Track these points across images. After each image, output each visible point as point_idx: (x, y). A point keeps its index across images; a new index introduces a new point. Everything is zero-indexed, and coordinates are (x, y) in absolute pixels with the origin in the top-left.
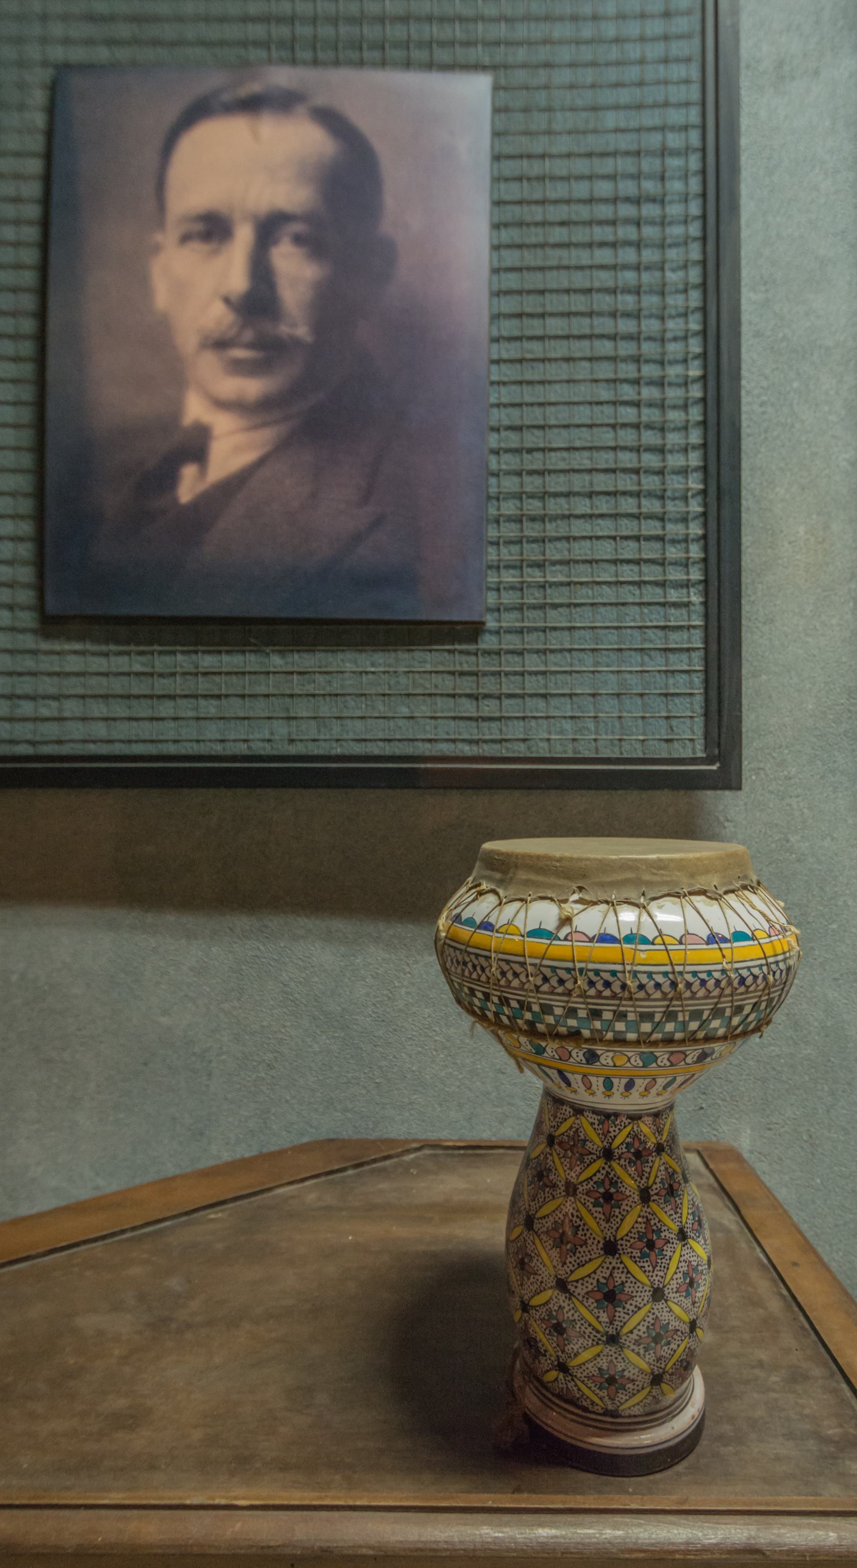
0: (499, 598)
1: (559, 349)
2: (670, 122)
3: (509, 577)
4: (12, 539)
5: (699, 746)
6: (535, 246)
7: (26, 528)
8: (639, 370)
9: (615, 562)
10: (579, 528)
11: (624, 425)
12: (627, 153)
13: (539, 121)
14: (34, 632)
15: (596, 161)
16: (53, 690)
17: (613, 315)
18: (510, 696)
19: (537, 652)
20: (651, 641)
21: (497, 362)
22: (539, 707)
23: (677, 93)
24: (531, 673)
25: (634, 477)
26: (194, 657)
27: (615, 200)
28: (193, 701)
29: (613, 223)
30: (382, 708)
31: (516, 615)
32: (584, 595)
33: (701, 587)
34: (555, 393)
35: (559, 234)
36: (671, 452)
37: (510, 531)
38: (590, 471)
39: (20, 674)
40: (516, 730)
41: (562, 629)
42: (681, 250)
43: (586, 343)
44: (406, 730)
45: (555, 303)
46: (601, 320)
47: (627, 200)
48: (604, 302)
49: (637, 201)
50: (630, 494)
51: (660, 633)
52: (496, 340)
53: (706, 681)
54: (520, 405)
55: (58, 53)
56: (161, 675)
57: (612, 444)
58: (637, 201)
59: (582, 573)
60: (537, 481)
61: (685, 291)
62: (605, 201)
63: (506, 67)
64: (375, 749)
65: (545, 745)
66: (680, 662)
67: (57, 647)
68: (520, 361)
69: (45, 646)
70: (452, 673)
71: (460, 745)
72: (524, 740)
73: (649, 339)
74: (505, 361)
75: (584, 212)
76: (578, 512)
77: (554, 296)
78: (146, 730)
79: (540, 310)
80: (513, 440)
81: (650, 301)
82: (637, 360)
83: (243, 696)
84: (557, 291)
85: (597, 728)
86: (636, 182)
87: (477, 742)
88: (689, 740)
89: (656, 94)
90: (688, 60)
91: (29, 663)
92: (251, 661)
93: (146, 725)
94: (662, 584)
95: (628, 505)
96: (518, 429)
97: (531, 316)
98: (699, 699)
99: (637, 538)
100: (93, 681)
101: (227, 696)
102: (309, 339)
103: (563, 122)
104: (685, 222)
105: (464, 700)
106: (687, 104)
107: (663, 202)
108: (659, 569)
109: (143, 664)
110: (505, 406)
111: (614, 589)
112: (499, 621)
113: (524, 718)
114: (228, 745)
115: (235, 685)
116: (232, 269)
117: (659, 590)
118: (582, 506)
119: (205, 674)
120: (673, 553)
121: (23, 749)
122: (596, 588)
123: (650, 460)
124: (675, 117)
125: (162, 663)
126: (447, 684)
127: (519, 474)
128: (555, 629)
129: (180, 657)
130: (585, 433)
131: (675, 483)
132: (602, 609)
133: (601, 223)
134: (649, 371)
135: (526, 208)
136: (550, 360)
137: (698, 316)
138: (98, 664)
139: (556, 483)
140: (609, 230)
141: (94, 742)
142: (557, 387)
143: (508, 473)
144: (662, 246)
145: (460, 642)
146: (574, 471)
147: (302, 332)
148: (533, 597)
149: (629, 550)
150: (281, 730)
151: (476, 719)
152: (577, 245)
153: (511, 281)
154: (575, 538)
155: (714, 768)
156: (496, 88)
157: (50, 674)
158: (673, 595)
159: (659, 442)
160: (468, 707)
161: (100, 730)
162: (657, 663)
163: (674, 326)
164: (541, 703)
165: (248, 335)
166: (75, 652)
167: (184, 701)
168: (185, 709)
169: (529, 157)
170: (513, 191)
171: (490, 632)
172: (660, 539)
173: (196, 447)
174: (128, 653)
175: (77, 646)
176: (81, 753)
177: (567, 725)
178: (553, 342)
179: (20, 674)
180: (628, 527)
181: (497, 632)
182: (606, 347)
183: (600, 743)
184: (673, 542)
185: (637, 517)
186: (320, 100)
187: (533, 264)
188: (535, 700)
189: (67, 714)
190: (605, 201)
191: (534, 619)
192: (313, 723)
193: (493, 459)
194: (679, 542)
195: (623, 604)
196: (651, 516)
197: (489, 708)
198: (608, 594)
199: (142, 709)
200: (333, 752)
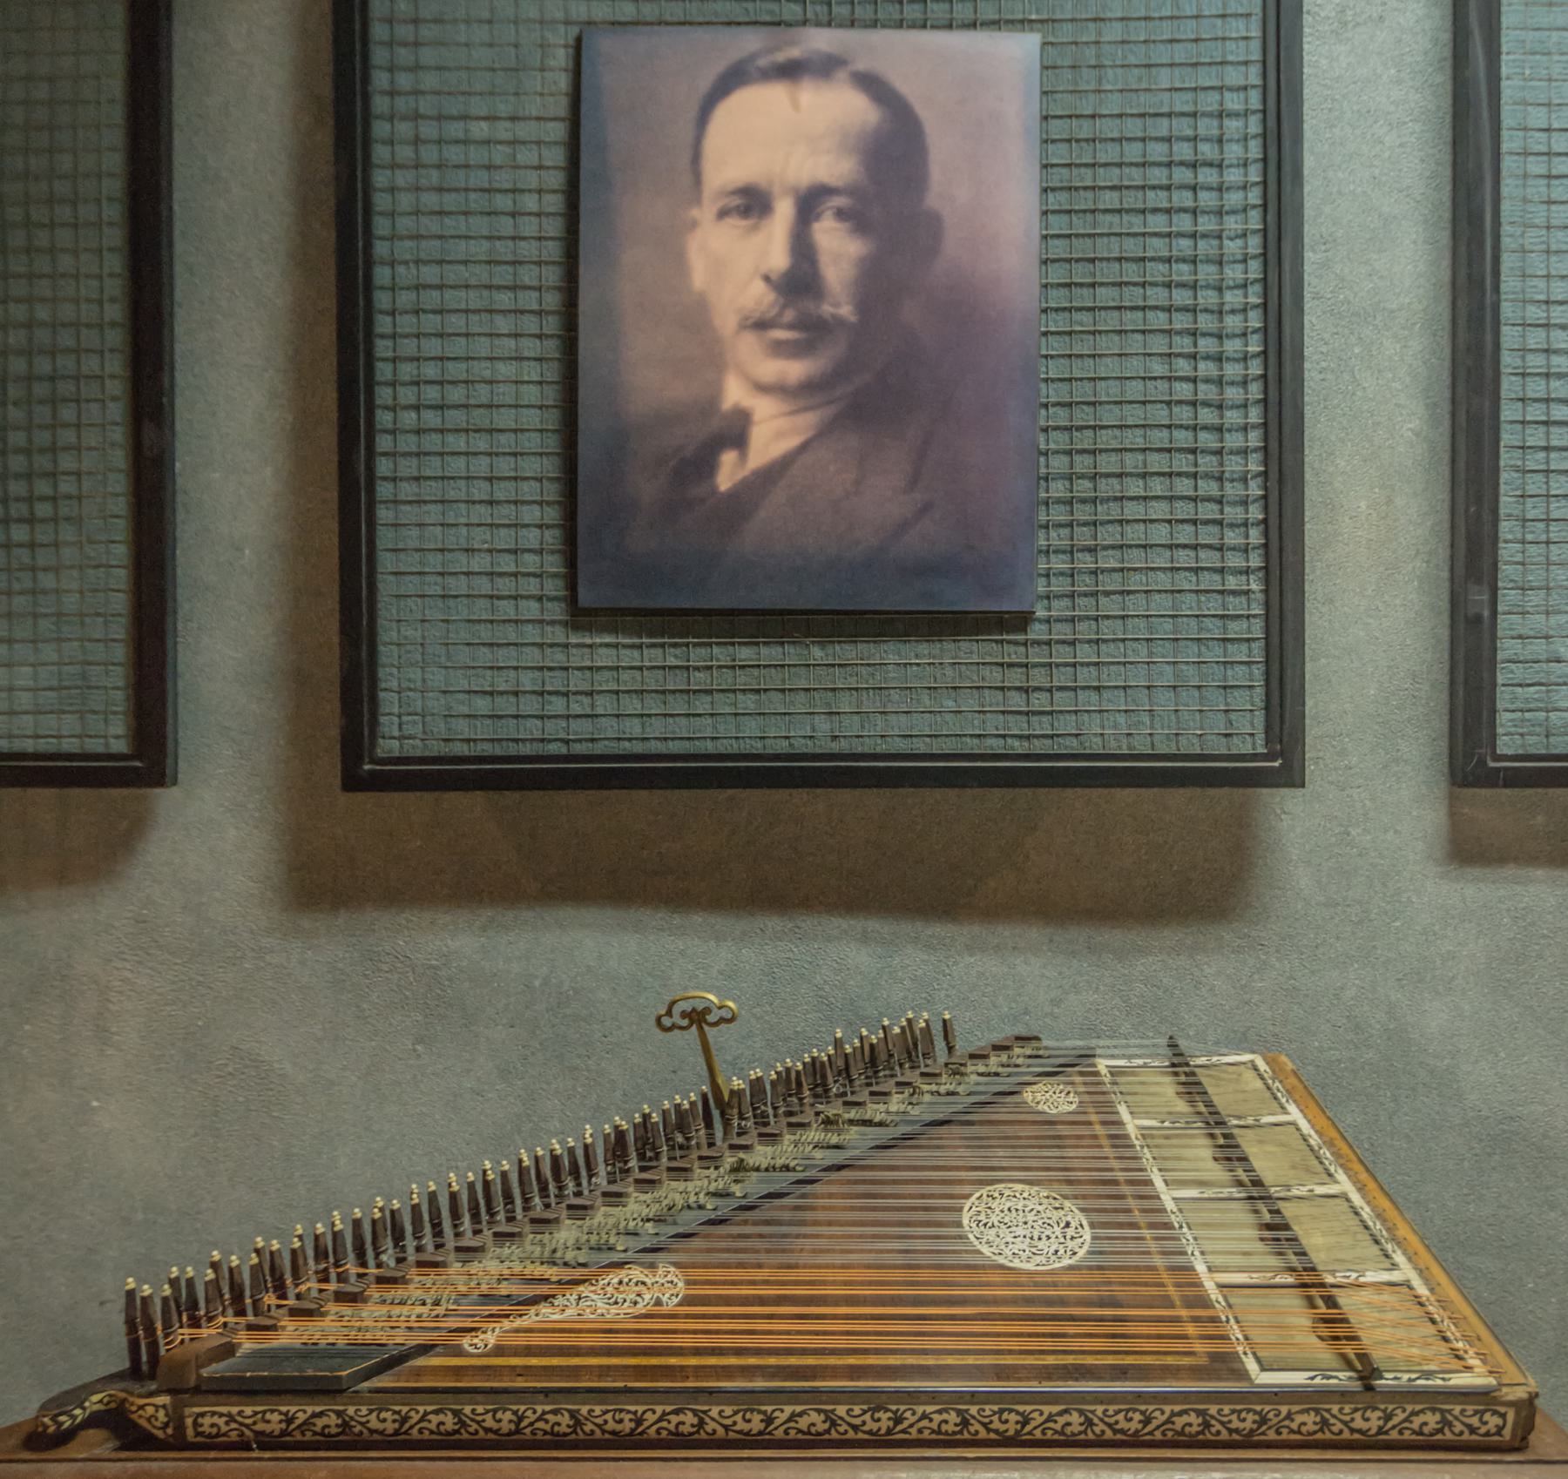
0: (1049, 585)
1: (1111, 321)
2: (1228, 82)
3: (1059, 563)
4: (540, 527)
5: (1260, 740)
6: (1084, 211)
7: (552, 515)
8: (1195, 345)
9: (1170, 547)
10: (1133, 510)
11: (1180, 402)
12: (1183, 114)
13: (1088, 80)
14: (565, 624)
15: (1149, 121)
16: (586, 687)
17: (1168, 285)
18: (1060, 689)
19: (1089, 641)
20: (1209, 631)
21: (1045, 334)
22: (1088, 700)
23: (1236, 52)
24: (1082, 664)
25: (1190, 457)
26: (731, 648)
27: (1169, 165)
28: (731, 695)
29: (1168, 188)
30: (928, 703)
31: (1066, 602)
32: (1136, 582)
33: (1261, 574)
34: (1108, 367)
35: (1110, 199)
36: (1229, 431)
37: (1059, 514)
38: (1144, 450)
39: (550, 669)
40: (1067, 725)
41: (1115, 617)
42: (1240, 217)
43: (1140, 314)
44: (952, 725)
45: (1109, 272)
46: (1155, 290)
47: (1182, 163)
48: (1157, 271)
49: (1194, 166)
50: (1186, 475)
51: (1219, 623)
52: (1044, 311)
53: (1267, 674)
54: (1070, 380)
55: (580, 11)
56: (697, 669)
57: (1167, 422)
58: (1194, 166)
59: (1136, 559)
60: (1088, 460)
61: (1245, 261)
62: (1159, 164)
63: (1054, 21)
64: (920, 746)
65: (1099, 740)
66: (1239, 653)
67: (588, 641)
68: (1070, 333)
69: (573, 640)
70: (1002, 665)
71: (1009, 741)
72: (1077, 735)
73: (1206, 310)
74: (1052, 333)
75: (1135, 176)
76: (1131, 494)
77: (1105, 264)
78: (682, 727)
79: (1090, 280)
80: (1061, 417)
81: (1207, 272)
82: (1194, 334)
83: (783, 691)
84: (1108, 259)
85: (1152, 721)
86: (1192, 144)
87: (1028, 737)
88: (1248, 736)
89: (1214, 52)
90: (1249, 15)
91: (559, 657)
92: (791, 653)
93: (683, 721)
94: (1221, 571)
95: (1183, 486)
96: (1070, 405)
97: (1081, 285)
98: (1259, 692)
99: (1194, 522)
100: (625, 676)
101: (766, 690)
102: (853, 319)
103: (1113, 80)
104: (1244, 188)
105: (1013, 693)
106: (1246, 63)
107: (1220, 166)
108: (1218, 554)
109: (676, 656)
110: (1053, 380)
111: (1169, 574)
112: (1049, 609)
113: (1076, 712)
114: (768, 742)
115: (775, 679)
116: (772, 246)
117: (1217, 577)
118: (1135, 487)
119: (743, 667)
120: (1232, 537)
121: (554, 748)
122: (1150, 574)
123: (1207, 439)
124: (1234, 76)
125: (698, 656)
126: (995, 676)
127: (1069, 453)
128: (1108, 617)
129: (716, 650)
130: (1138, 411)
131: (1233, 465)
132: (1157, 596)
133: (1154, 188)
134: (1206, 345)
135: (1075, 171)
136: (1100, 332)
137: (1258, 288)
138: (629, 657)
139: (1107, 463)
140: (1163, 194)
141: (630, 740)
142: (1109, 360)
143: (1057, 452)
144: (1220, 213)
145: (1008, 633)
146: (1126, 450)
147: (846, 311)
148: (1085, 584)
149: (1185, 534)
150: (823, 726)
151: (1027, 713)
152: (1128, 211)
153: (1059, 248)
154: (1128, 521)
155: (1276, 764)
156: (1044, 44)
157: (579, 669)
158: (1232, 582)
159: (1217, 421)
160: (1017, 701)
161: (634, 728)
162: (1215, 654)
163: (1233, 298)
164: (1094, 696)
165: (789, 315)
166: (607, 645)
167: (721, 695)
168: (723, 705)
169: (1077, 116)
170: (1059, 154)
171: (1040, 621)
172: (1220, 523)
173: (736, 433)
174: (662, 646)
175: (608, 639)
176: (616, 752)
177: (1121, 719)
178: (1103, 313)
179: (550, 669)
180: (1184, 510)
181: (1048, 621)
182: (1158, 320)
183: (1156, 738)
184: (1232, 526)
185: (1194, 499)
186: (861, 65)
187: (1082, 231)
188: (1087, 693)
189: (600, 711)
190: (1159, 164)
191: (1085, 606)
192: (856, 718)
193: (1042, 438)
194: (1238, 526)
195: (1179, 591)
196: (1209, 499)
197: (1039, 701)
198: (1163, 580)
199: (678, 705)
200: (878, 750)
